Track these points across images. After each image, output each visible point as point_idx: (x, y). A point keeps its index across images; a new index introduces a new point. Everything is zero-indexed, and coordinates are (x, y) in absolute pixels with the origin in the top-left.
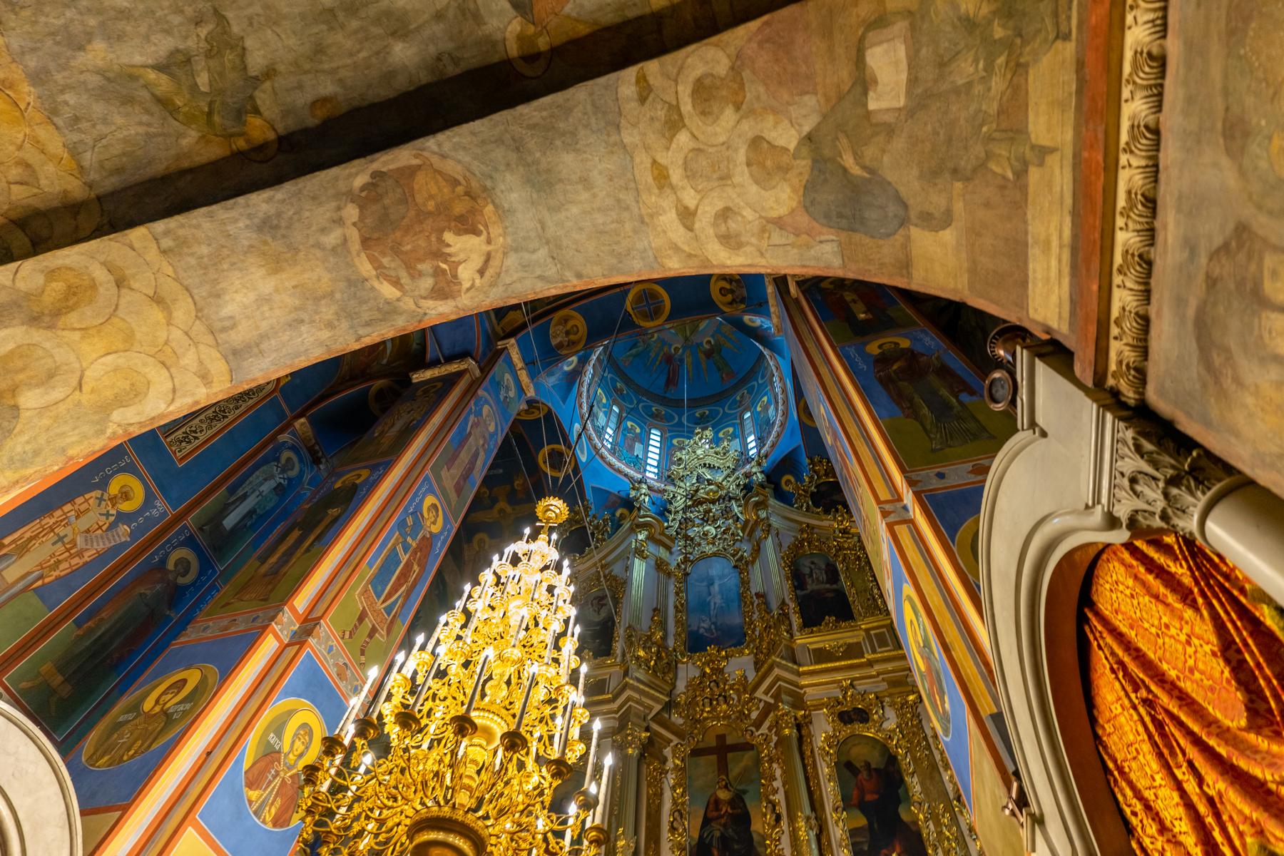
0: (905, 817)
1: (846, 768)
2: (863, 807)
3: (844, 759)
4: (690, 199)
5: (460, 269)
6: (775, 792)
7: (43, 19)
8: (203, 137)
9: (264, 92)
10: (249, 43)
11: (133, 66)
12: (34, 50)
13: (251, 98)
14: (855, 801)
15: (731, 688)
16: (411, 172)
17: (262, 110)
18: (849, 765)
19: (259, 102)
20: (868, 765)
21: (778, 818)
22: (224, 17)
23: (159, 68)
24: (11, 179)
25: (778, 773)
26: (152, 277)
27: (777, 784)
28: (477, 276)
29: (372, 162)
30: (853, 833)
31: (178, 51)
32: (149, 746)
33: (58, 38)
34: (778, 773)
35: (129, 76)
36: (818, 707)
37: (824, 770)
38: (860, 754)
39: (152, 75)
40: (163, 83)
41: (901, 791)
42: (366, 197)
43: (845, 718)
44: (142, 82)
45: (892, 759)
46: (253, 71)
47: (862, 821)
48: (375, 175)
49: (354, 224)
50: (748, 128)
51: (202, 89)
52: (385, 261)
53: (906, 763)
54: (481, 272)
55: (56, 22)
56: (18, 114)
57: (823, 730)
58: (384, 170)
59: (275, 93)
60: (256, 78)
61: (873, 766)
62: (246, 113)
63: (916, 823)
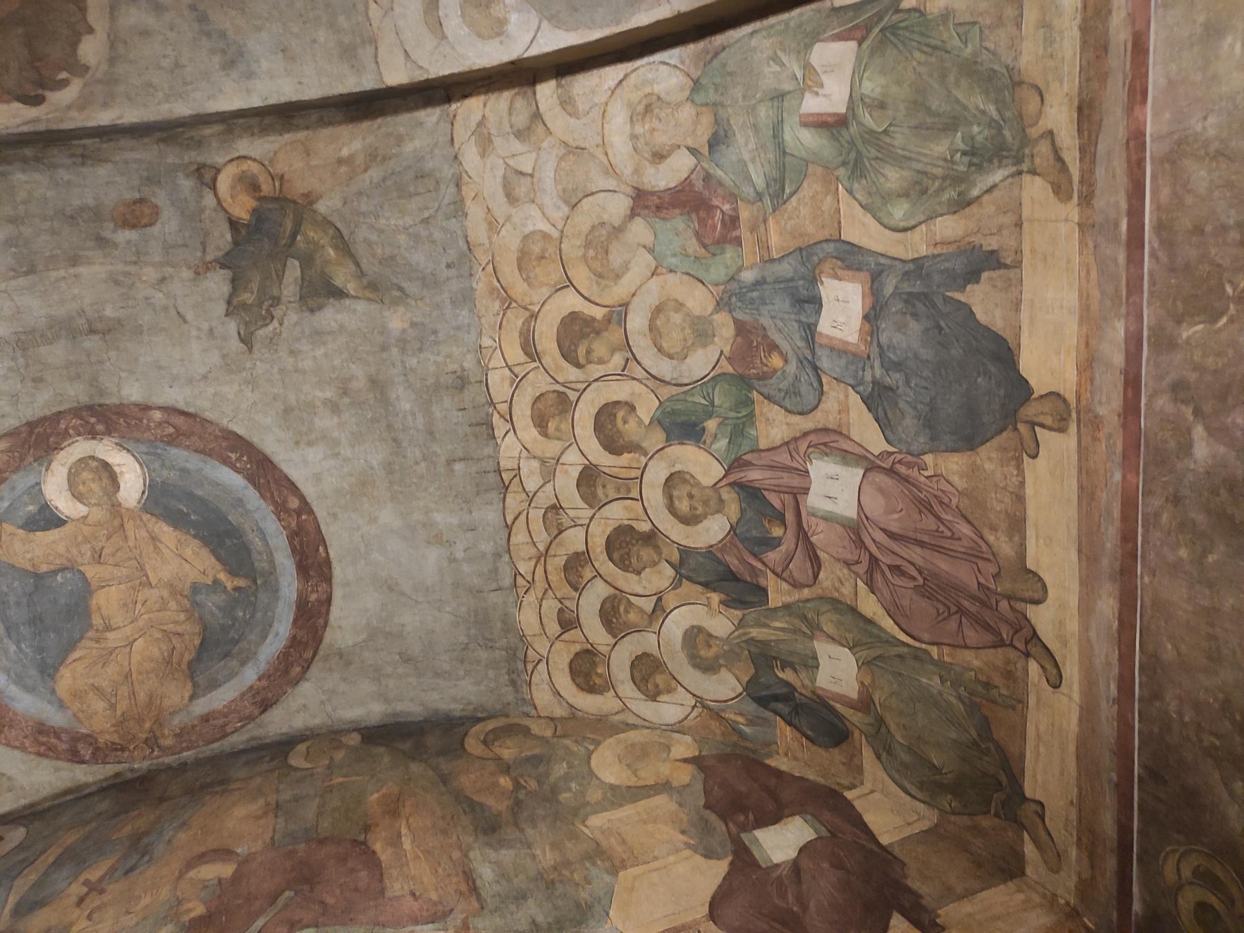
7: (440, 359)
8: (311, 203)
9: (218, 248)
10: (221, 308)
11: (369, 300)
12: (458, 328)
13: (236, 243)
17: (226, 226)
19: (229, 237)
22: (242, 341)
23: (339, 294)
24: (529, 178)
26: (395, 6)
29: (37, 120)
31: (312, 311)
33: (433, 338)
35: (374, 288)
39: (351, 287)
40: (342, 276)
42: (62, 69)
44: (365, 281)
46: (227, 273)
48: (37, 101)
49: (91, 30)
51: (297, 263)
55: (430, 356)
56: (497, 259)
58: (17, 105)
59: (204, 245)
60: (223, 266)
62: (248, 226)
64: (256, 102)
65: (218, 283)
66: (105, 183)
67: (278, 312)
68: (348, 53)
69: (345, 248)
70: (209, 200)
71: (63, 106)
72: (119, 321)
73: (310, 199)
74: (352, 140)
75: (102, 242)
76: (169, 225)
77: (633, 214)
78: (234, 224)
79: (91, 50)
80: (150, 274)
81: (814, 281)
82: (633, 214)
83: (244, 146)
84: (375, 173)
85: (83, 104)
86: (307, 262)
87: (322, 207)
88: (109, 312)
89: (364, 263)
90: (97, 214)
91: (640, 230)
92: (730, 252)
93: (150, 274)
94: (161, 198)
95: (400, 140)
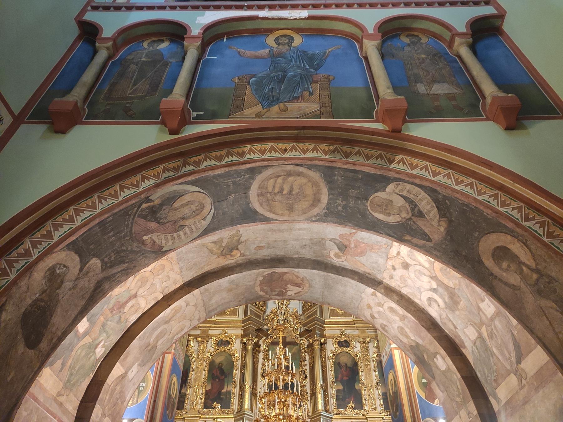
0: (357, 387)
1: (337, 365)
2: (342, 382)
3: (338, 361)
4: (376, 316)
5: (288, 292)
6: (306, 365)
14: (339, 379)
15: (291, 316)
16: (286, 273)
18: (339, 364)
20: (346, 365)
21: (306, 377)
25: (307, 358)
27: (307, 362)
28: (293, 294)
30: (337, 391)
32: (137, 401)
34: (307, 358)
36: (329, 337)
37: (330, 365)
38: (344, 360)
39: (210, 244)
41: (357, 377)
43: (340, 344)
45: (356, 364)
47: (341, 387)
50: (401, 324)
52: (265, 288)
53: (361, 365)
54: (295, 294)
57: (331, 347)
61: (349, 366)
63: (360, 390)
64: (228, 277)
65: (242, 239)
66: (264, 253)
67: (229, 236)
68: (206, 290)
69: (211, 251)
70: (242, 252)
71: (267, 271)
72: (268, 231)
73: (218, 257)
74: (207, 268)
75: (269, 244)
76: (252, 247)
77: (136, 293)
78: (238, 249)
79: (261, 278)
80: (259, 239)
81: (91, 323)
82: (136, 293)
83: (233, 261)
84: (202, 265)
85: (265, 272)
86: (221, 246)
87: (216, 256)
88: (270, 233)
89: (206, 249)
90: (268, 247)
91: (133, 292)
92: (111, 306)
93: (259, 239)
94: (253, 251)
95: (196, 272)
